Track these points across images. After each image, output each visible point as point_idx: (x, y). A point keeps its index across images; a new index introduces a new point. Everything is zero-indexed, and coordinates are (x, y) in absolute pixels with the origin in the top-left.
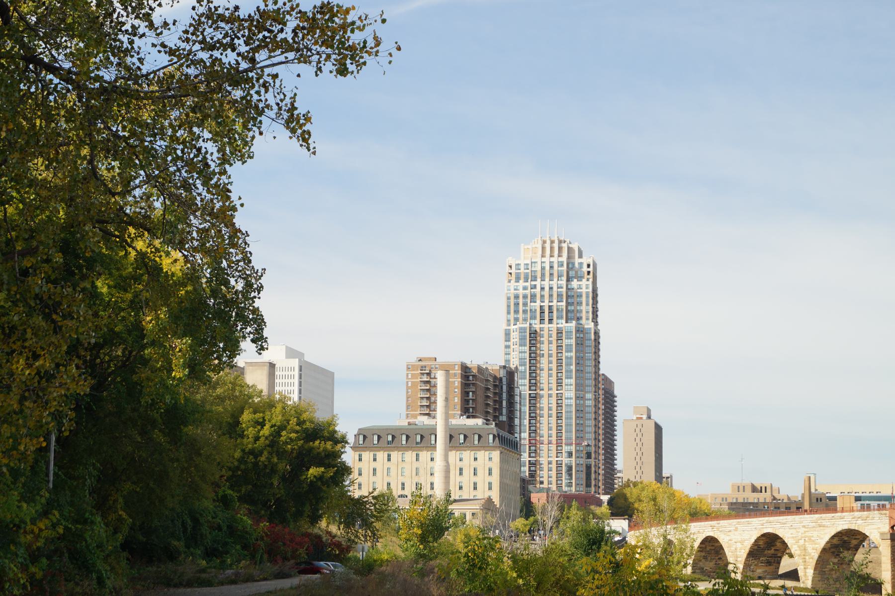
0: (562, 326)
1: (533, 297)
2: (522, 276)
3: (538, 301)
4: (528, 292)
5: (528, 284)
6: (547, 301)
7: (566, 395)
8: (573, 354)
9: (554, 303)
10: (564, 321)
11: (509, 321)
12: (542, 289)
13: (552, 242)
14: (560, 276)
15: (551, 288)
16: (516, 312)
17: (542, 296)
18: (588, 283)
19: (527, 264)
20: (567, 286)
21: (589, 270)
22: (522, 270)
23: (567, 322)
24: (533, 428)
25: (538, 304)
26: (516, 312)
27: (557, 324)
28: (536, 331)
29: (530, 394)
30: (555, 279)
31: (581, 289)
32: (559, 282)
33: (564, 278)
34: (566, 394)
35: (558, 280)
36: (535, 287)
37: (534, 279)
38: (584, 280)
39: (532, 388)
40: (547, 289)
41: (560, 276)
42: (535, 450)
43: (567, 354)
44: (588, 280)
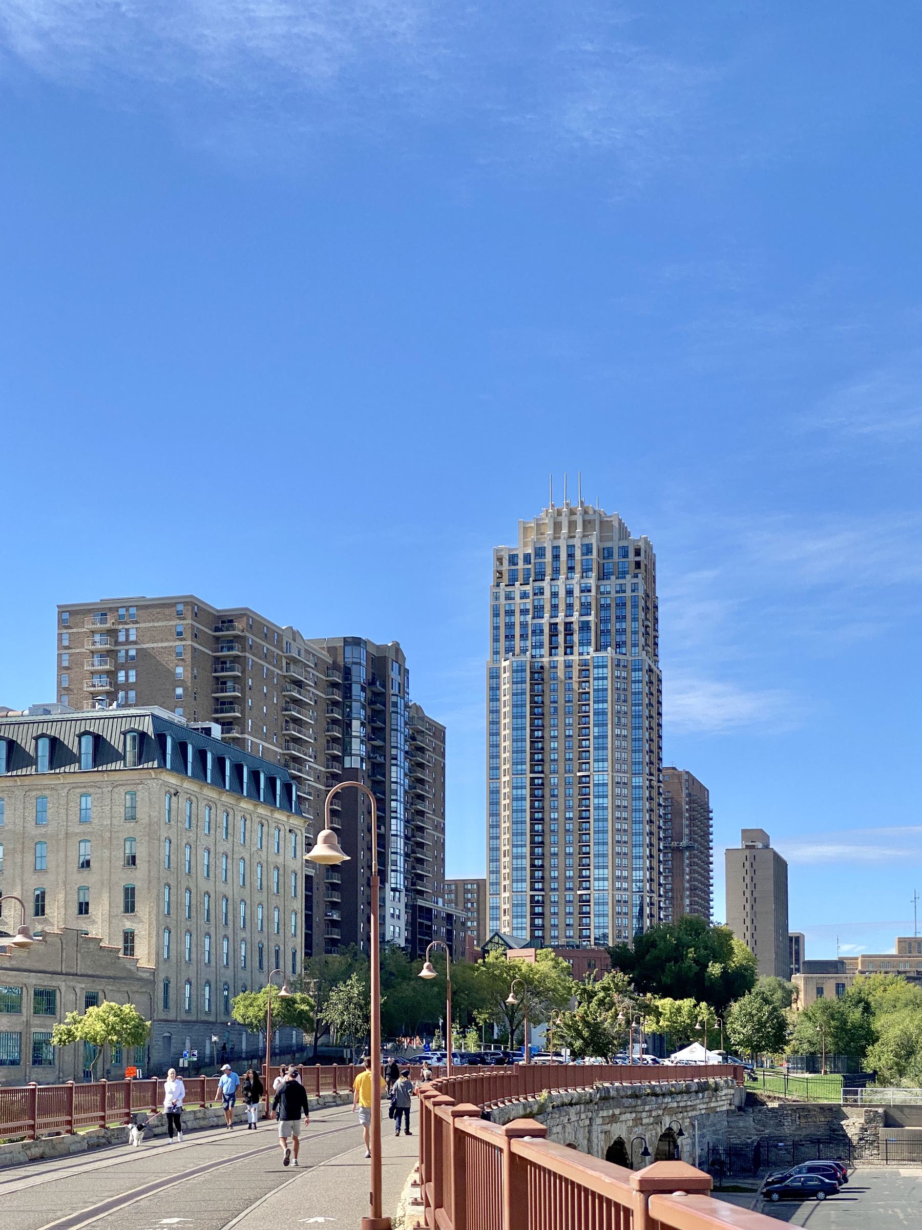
0: (589, 657)
1: (538, 611)
2: (521, 577)
3: (547, 615)
4: (529, 604)
5: (528, 588)
6: (561, 615)
7: (596, 778)
8: (608, 706)
9: (575, 618)
10: (591, 649)
11: (496, 653)
12: (555, 595)
13: (572, 513)
14: (586, 571)
15: (569, 593)
16: (510, 637)
17: (555, 607)
18: (635, 580)
19: (529, 555)
20: (598, 587)
21: (637, 559)
22: (521, 565)
23: (596, 650)
24: (538, 839)
25: (545, 621)
26: (510, 637)
27: (581, 654)
28: (542, 668)
29: (532, 779)
30: (577, 576)
31: (624, 592)
32: (585, 581)
33: (594, 574)
34: (596, 778)
35: (582, 577)
36: (541, 592)
37: (540, 577)
38: (628, 577)
39: (536, 768)
40: (562, 593)
41: (586, 571)
42: (543, 878)
43: (596, 706)
44: (636, 576)
